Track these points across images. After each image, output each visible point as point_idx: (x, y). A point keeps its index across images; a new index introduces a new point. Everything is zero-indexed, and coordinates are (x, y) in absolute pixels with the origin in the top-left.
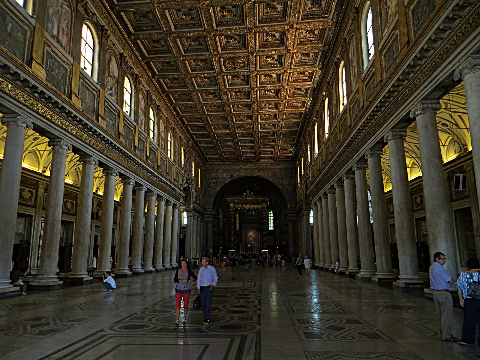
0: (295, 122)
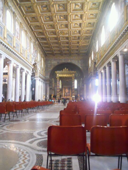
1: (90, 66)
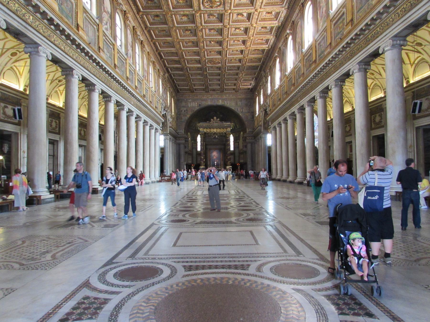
0: (258, 57)
1: (257, 113)
